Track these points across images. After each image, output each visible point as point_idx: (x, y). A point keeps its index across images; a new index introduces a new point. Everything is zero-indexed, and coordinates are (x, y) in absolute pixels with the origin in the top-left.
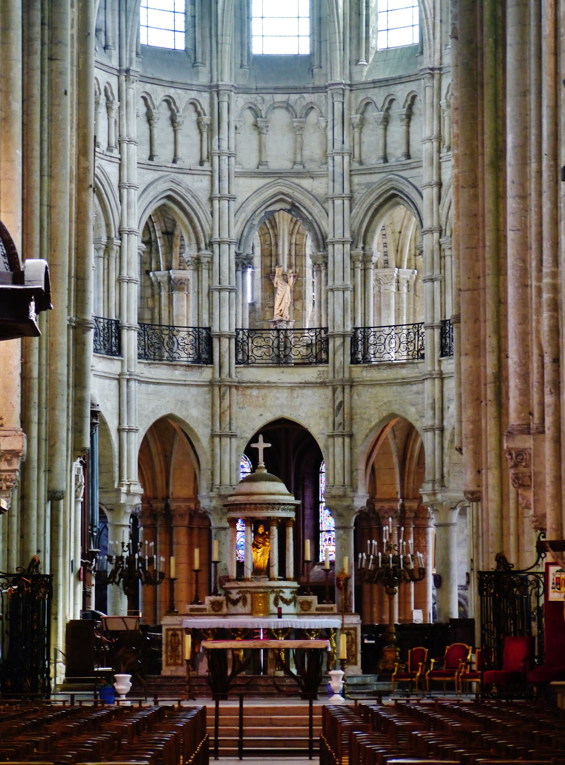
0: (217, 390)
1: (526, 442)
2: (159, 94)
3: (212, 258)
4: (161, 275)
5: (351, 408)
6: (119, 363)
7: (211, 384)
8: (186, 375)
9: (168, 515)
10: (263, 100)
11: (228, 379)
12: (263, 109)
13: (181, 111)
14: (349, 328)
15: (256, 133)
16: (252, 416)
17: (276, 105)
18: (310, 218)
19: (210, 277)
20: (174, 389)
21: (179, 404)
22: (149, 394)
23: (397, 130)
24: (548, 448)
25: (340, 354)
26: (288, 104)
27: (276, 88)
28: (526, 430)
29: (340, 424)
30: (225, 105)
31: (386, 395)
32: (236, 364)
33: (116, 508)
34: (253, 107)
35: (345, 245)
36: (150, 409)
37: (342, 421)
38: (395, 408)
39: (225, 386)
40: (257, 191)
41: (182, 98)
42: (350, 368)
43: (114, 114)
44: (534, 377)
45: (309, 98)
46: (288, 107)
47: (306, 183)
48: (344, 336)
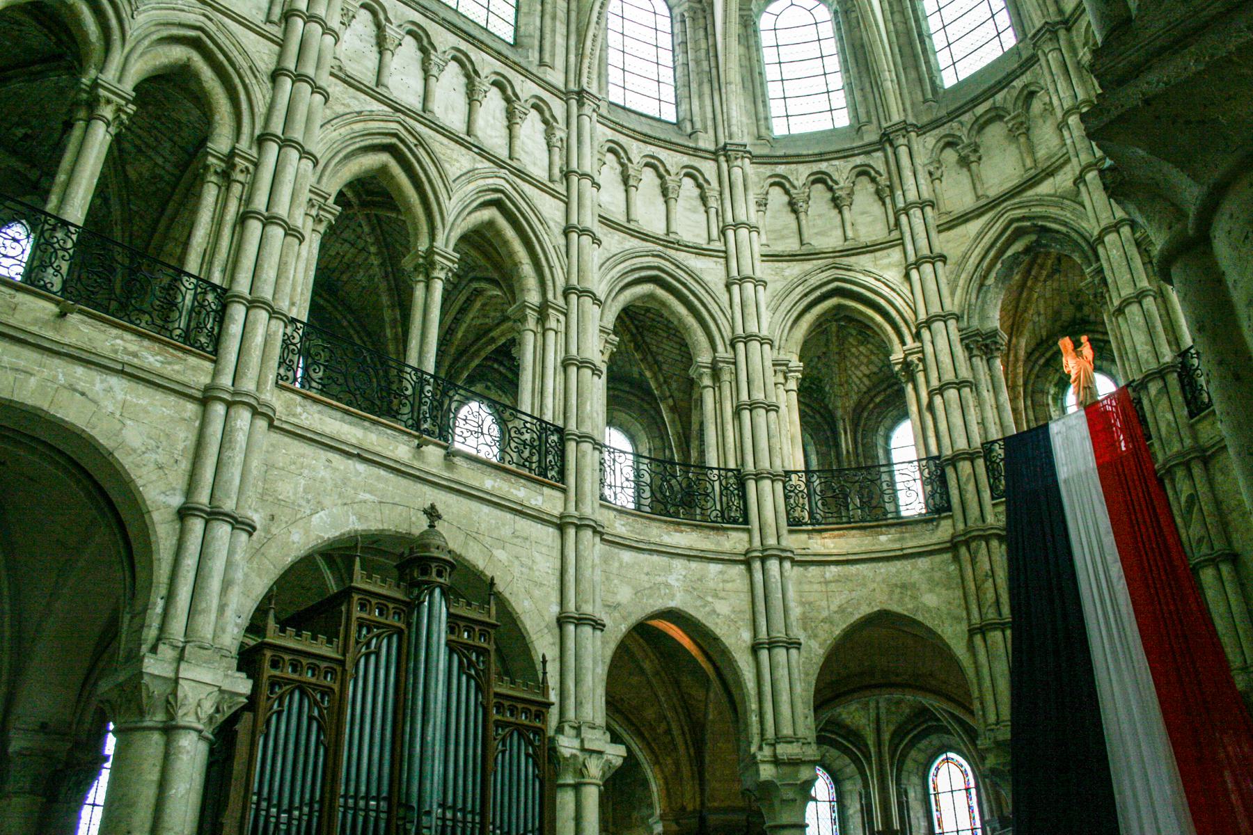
0: (963, 550)
3: (922, 351)
5: (1218, 503)
6: (745, 536)
7: (953, 547)
8: (902, 539)
10: (961, 123)
11: (980, 524)
12: (963, 134)
13: (842, 184)
14: (1168, 356)
15: (965, 170)
17: (982, 121)
18: (1064, 229)
19: (927, 382)
20: (883, 568)
21: (899, 590)
22: (827, 583)
26: (996, 108)
27: (972, 100)
29: (1200, 541)
30: (903, 151)
32: (993, 498)
34: (950, 139)
35: (1122, 230)
36: (834, 608)
37: (1203, 532)
39: (975, 538)
40: (981, 234)
42: (1192, 426)
43: (713, 203)
45: (1018, 84)
47: (1045, 188)
48: (1161, 373)
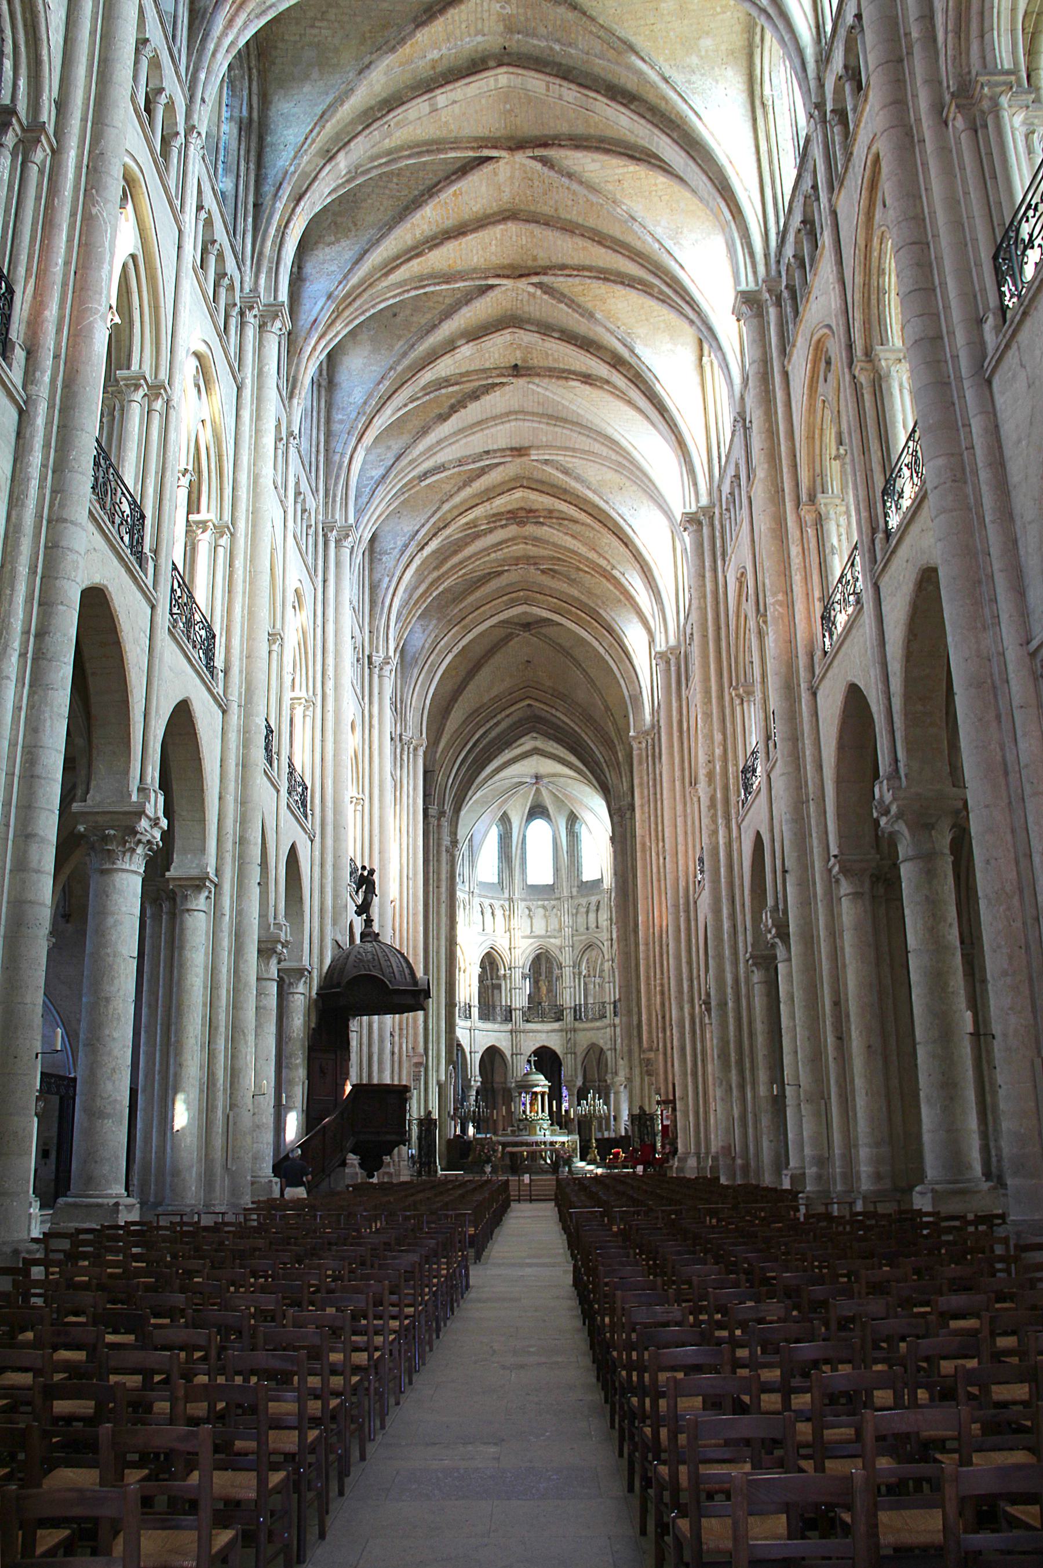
1: (652, 1055)
2: (486, 902)
4: (489, 982)
7: (511, 1032)
9: (493, 1090)
16: (530, 1045)
23: (592, 916)
24: (661, 1057)
25: (569, 1016)
28: (651, 1049)
31: (589, 1034)
33: (471, 1087)
38: (594, 1040)
41: (497, 904)
44: (654, 1025)
46: (544, 907)
